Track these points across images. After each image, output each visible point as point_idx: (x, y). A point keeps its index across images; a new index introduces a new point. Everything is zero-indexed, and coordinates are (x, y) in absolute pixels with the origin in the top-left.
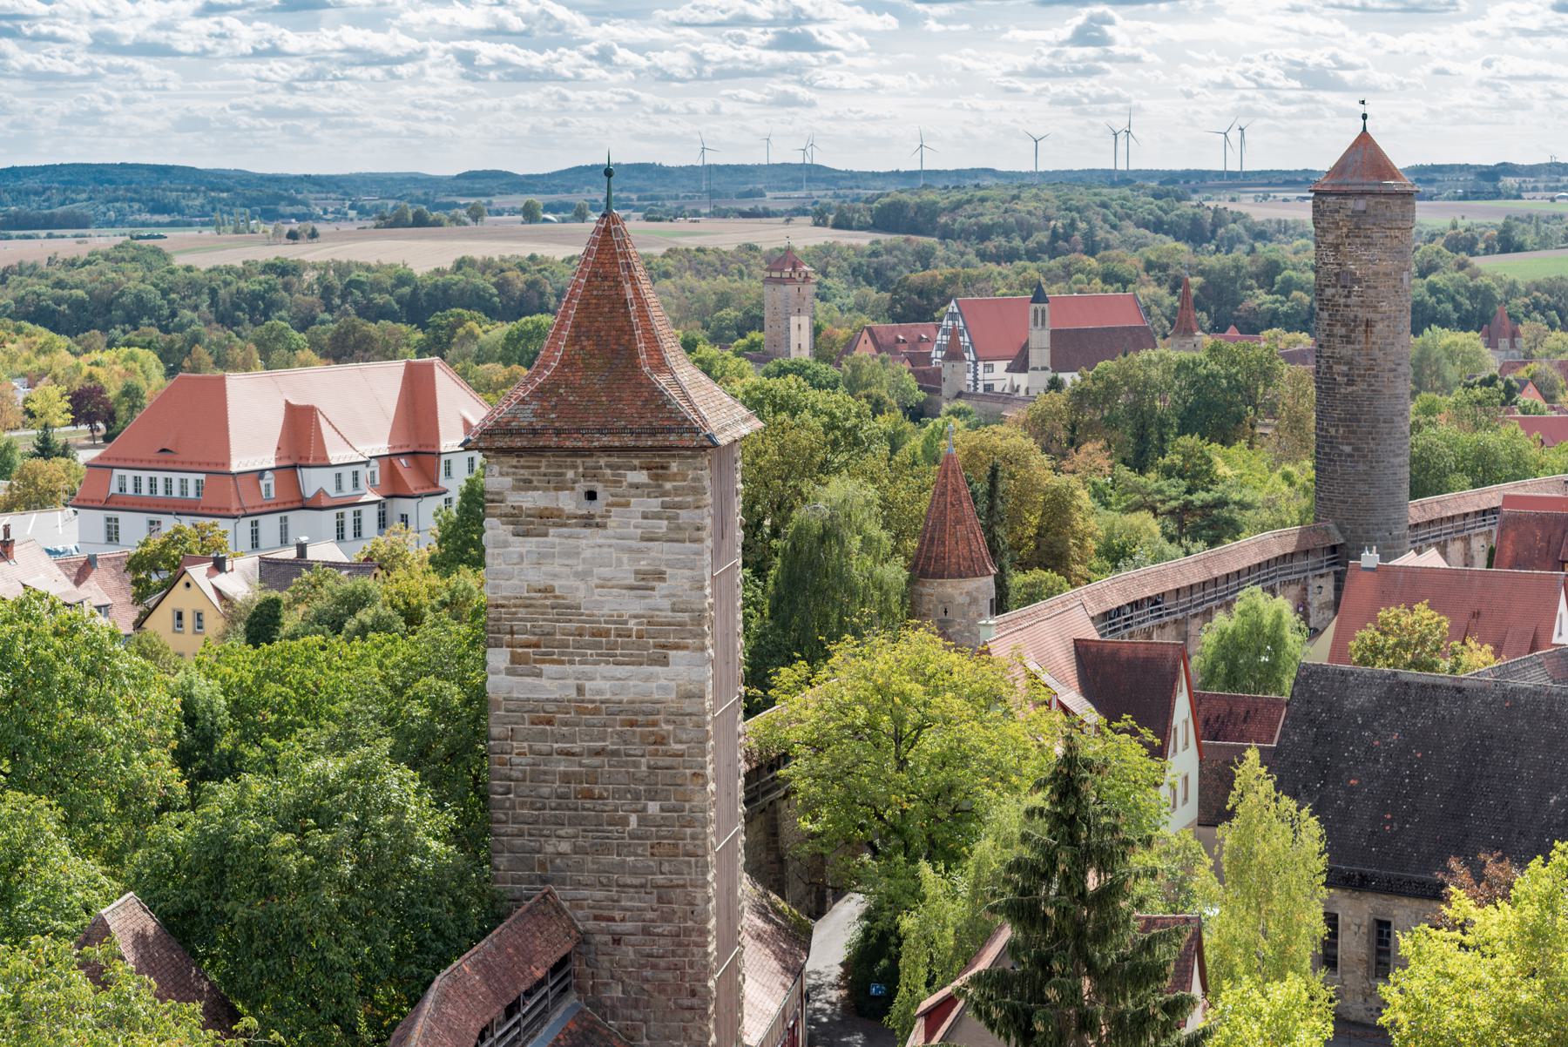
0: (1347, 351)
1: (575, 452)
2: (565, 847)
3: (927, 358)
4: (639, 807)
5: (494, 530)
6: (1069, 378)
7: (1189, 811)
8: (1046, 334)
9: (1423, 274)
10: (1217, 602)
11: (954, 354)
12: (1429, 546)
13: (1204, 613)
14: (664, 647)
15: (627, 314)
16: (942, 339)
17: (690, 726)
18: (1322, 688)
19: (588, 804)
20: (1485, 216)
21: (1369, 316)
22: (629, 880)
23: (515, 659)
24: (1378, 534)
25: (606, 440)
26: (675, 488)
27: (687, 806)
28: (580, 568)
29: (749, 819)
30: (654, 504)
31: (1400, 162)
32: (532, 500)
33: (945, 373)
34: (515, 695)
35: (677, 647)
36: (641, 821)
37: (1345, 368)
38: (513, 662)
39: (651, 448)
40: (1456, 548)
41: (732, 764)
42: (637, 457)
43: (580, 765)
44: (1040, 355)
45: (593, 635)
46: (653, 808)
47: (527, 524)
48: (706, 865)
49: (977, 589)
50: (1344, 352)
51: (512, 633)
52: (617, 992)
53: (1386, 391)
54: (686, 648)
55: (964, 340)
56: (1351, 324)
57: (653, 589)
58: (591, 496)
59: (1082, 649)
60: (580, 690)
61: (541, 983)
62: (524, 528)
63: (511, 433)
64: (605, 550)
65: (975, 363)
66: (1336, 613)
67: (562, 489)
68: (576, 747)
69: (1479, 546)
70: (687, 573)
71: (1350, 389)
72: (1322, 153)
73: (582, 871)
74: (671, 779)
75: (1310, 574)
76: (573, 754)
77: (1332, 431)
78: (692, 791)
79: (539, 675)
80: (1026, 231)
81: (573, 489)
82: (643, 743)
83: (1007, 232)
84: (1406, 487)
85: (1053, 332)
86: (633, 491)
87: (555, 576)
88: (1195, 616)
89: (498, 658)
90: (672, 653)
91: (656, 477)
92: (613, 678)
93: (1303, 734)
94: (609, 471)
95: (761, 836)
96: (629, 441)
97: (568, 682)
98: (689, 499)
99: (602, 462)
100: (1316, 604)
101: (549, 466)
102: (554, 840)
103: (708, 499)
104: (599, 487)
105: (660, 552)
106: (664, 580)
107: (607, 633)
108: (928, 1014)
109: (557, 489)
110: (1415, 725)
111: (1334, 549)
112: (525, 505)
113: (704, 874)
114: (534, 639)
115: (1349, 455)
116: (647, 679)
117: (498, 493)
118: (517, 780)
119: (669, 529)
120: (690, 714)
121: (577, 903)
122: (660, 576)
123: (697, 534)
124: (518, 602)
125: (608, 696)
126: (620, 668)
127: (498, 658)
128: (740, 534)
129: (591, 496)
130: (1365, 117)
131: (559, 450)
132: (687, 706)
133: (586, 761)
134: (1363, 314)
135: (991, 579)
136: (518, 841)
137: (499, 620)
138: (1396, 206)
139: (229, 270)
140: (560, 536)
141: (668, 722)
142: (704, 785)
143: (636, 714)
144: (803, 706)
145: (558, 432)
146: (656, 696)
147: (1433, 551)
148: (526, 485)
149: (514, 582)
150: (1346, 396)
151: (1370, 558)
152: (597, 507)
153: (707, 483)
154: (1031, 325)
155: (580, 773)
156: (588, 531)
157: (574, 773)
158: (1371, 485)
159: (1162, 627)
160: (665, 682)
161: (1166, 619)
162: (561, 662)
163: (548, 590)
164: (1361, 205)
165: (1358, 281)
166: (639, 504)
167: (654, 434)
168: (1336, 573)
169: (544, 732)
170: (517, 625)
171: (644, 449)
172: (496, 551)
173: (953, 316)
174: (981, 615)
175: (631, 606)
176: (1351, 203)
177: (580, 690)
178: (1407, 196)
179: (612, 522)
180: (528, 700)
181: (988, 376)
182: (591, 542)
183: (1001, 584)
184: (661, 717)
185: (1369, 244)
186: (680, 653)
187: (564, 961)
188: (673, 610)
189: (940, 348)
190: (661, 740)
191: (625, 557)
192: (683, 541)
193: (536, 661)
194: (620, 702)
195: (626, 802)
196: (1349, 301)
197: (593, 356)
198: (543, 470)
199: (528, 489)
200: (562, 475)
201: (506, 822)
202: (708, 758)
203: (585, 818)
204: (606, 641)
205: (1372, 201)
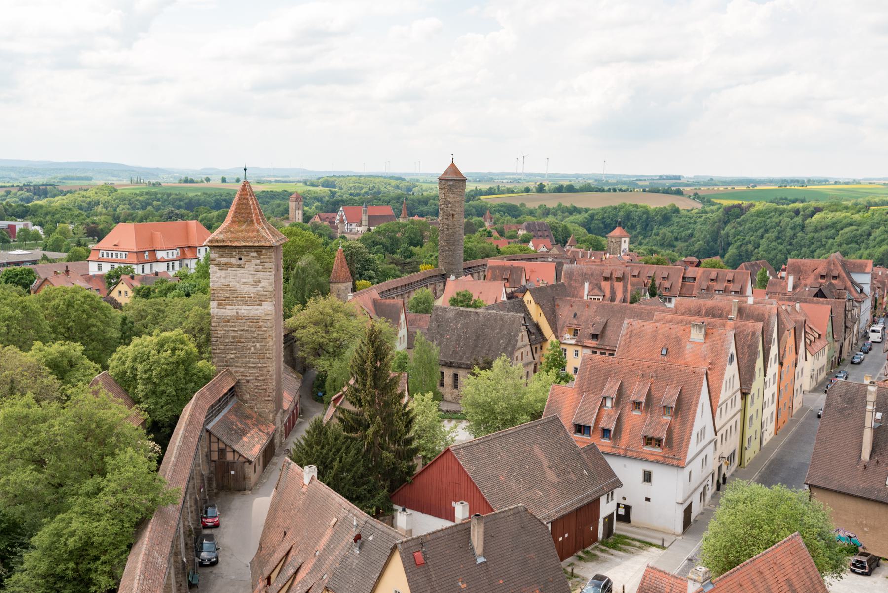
0: (447, 222)
1: (236, 247)
2: (233, 356)
3: (334, 222)
5: (212, 269)
6: (373, 228)
7: (405, 345)
9: (467, 201)
11: (342, 222)
16: (338, 217)
20: (484, 187)
23: (219, 305)
29: (285, 348)
30: (258, 262)
32: (224, 260)
33: (339, 226)
41: (280, 333)
44: (364, 222)
46: (258, 345)
47: (222, 267)
52: (248, 396)
55: (344, 218)
58: (240, 259)
59: (375, 302)
61: (226, 394)
63: (217, 242)
72: (441, 169)
74: (261, 338)
80: (362, 188)
89: (213, 304)
104: (243, 257)
105: (260, 275)
108: (334, 400)
121: (236, 372)
122: (260, 282)
127: (213, 304)
129: (240, 259)
131: (231, 246)
139: (136, 194)
144: (300, 316)
148: (222, 256)
151: (453, 278)
152: (241, 262)
163: (228, 285)
164: (451, 183)
166: (254, 262)
175: (252, 289)
178: (464, 180)
183: (354, 284)
187: (233, 388)
190: (260, 327)
204: (245, 299)
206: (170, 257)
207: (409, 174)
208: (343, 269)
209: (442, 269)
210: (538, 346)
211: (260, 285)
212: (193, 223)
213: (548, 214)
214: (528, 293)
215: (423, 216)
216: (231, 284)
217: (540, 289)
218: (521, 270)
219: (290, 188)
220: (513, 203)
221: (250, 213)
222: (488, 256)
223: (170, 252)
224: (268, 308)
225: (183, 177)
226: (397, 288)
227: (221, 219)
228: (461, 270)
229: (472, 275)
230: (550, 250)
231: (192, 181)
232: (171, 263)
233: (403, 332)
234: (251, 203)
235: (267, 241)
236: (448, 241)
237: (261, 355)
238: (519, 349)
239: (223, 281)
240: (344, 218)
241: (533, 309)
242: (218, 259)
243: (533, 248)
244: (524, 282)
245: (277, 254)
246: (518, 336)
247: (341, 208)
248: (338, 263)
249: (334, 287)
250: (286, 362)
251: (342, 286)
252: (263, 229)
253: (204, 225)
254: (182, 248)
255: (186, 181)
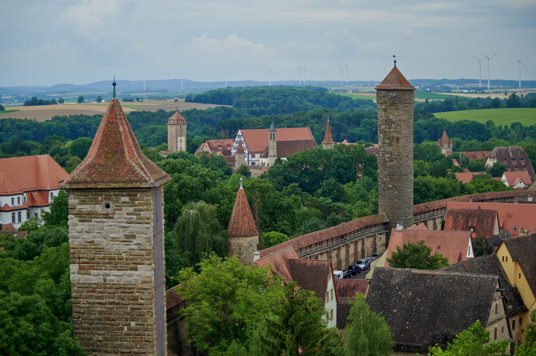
0: (390, 149)
1: (102, 190)
2: (100, 338)
3: (229, 152)
4: (128, 323)
8: (275, 143)
10: (342, 245)
11: (240, 151)
12: (421, 222)
13: (337, 249)
14: (136, 264)
15: (121, 137)
16: (235, 145)
17: (146, 293)
18: (383, 276)
19: (109, 322)
21: (398, 136)
22: (125, 350)
23: (81, 268)
24: (402, 218)
25: (113, 185)
26: (139, 204)
27: (146, 323)
28: (104, 234)
29: (168, 328)
31: (407, 80)
32: (87, 208)
34: (81, 282)
35: (141, 264)
36: (128, 329)
37: (389, 155)
38: (80, 269)
39: (130, 188)
40: (430, 223)
42: (125, 191)
43: (106, 308)
44: (273, 152)
45: (109, 259)
46: (133, 324)
48: (153, 345)
49: (252, 241)
50: (389, 150)
51: (79, 258)
53: (404, 164)
54: (144, 264)
55: (244, 145)
56: (391, 139)
57: (131, 242)
58: (108, 206)
60: (105, 280)
62: (83, 219)
63: (78, 183)
64: (113, 227)
65: (248, 154)
66: (387, 248)
67: (97, 204)
68: (104, 301)
69: (438, 221)
70: (144, 235)
71: (391, 163)
73: (107, 347)
74: (137, 314)
75: (377, 233)
76: (103, 304)
77: (385, 179)
78: (148, 318)
79: (89, 274)
80: (267, 104)
81: (101, 204)
82: (129, 300)
83: (258, 104)
84: (412, 200)
85: (279, 144)
86: (123, 205)
87: (95, 237)
88: (334, 250)
90: (139, 266)
91: (133, 200)
92: (117, 275)
93: (376, 294)
94: (114, 197)
95: (172, 334)
96: (121, 185)
97: (101, 277)
98: (145, 207)
99: (112, 193)
100: (379, 244)
101: (92, 195)
102: (96, 336)
103: (152, 207)
104: (111, 203)
105: (134, 228)
106: (135, 238)
107: (114, 259)
109: (95, 204)
110: (417, 289)
111: (385, 224)
112: (83, 210)
113: (152, 348)
114: (87, 260)
115: (391, 188)
116: (130, 276)
117: (73, 206)
118: (82, 313)
119: (137, 219)
120: (146, 289)
122: (134, 237)
123: (147, 221)
124: (81, 247)
125: (115, 282)
126: (119, 272)
128: (164, 220)
130: (395, 62)
132: (145, 286)
133: (107, 306)
134: (395, 135)
135: (257, 237)
136: (83, 336)
137: (74, 253)
138: (407, 96)
140: (96, 222)
141: (138, 292)
142: (152, 316)
143: (126, 289)
145: (95, 182)
146: (133, 282)
147: (422, 224)
148: (83, 202)
149: (80, 239)
150: (389, 166)
151: (399, 227)
152: (110, 210)
153: (152, 202)
154: (269, 140)
155: (105, 311)
156: (106, 220)
157: (103, 311)
158: (400, 200)
159: (322, 254)
160: (136, 277)
161: (323, 251)
162: (98, 270)
163: (92, 242)
164: (394, 94)
165: (394, 123)
167: (131, 183)
168: (386, 232)
169: (91, 296)
170: (81, 255)
171: (128, 188)
172: (73, 227)
173: (239, 136)
174: (253, 251)
175: (123, 248)
176: (391, 94)
177: (105, 280)
179: (115, 216)
180: (85, 283)
181: (253, 159)
182: (108, 224)
184: (135, 290)
185: (397, 109)
186: (142, 266)
188: (139, 250)
189: (235, 148)
190: (136, 299)
191: (121, 230)
192: (142, 223)
193: (88, 269)
194: (120, 284)
195: (123, 322)
196: (390, 130)
197: (108, 153)
198: (90, 196)
199: (84, 204)
200: (98, 198)
201: (78, 329)
202: (153, 305)
203: (107, 327)
204: (114, 261)
205: (398, 93)
206: (16, 204)
207: (334, 83)
208: (246, 219)
209: (383, 215)
210: (517, 319)
211: (135, 241)
212: (45, 159)
213: (524, 136)
214: (503, 246)
215: (353, 141)
216: (97, 240)
217: (519, 240)
218: (492, 214)
219: (168, 106)
220: (478, 121)
221: (120, 143)
222: (446, 196)
223: (16, 197)
224: (146, 273)
225: (30, 98)
226: (321, 243)
227: (81, 152)
228: (411, 216)
229: (425, 223)
230: (529, 185)
231: (41, 103)
232: (16, 213)
233: (331, 305)
234: (121, 129)
235: (142, 180)
236: (391, 175)
237: (137, 335)
238: (492, 323)
239: (86, 236)
240: (244, 145)
241: (510, 268)
242: (79, 207)
243: (507, 184)
244: (496, 232)
245: (156, 200)
246: (489, 306)
247: (240, 133)
248: (241, 212)
249: (234, 242)
250: (169, 347)
251: (244, 242)
252: (138, 164)
253: (57, 160)
254: (30, 192)
255: (35, 102)
